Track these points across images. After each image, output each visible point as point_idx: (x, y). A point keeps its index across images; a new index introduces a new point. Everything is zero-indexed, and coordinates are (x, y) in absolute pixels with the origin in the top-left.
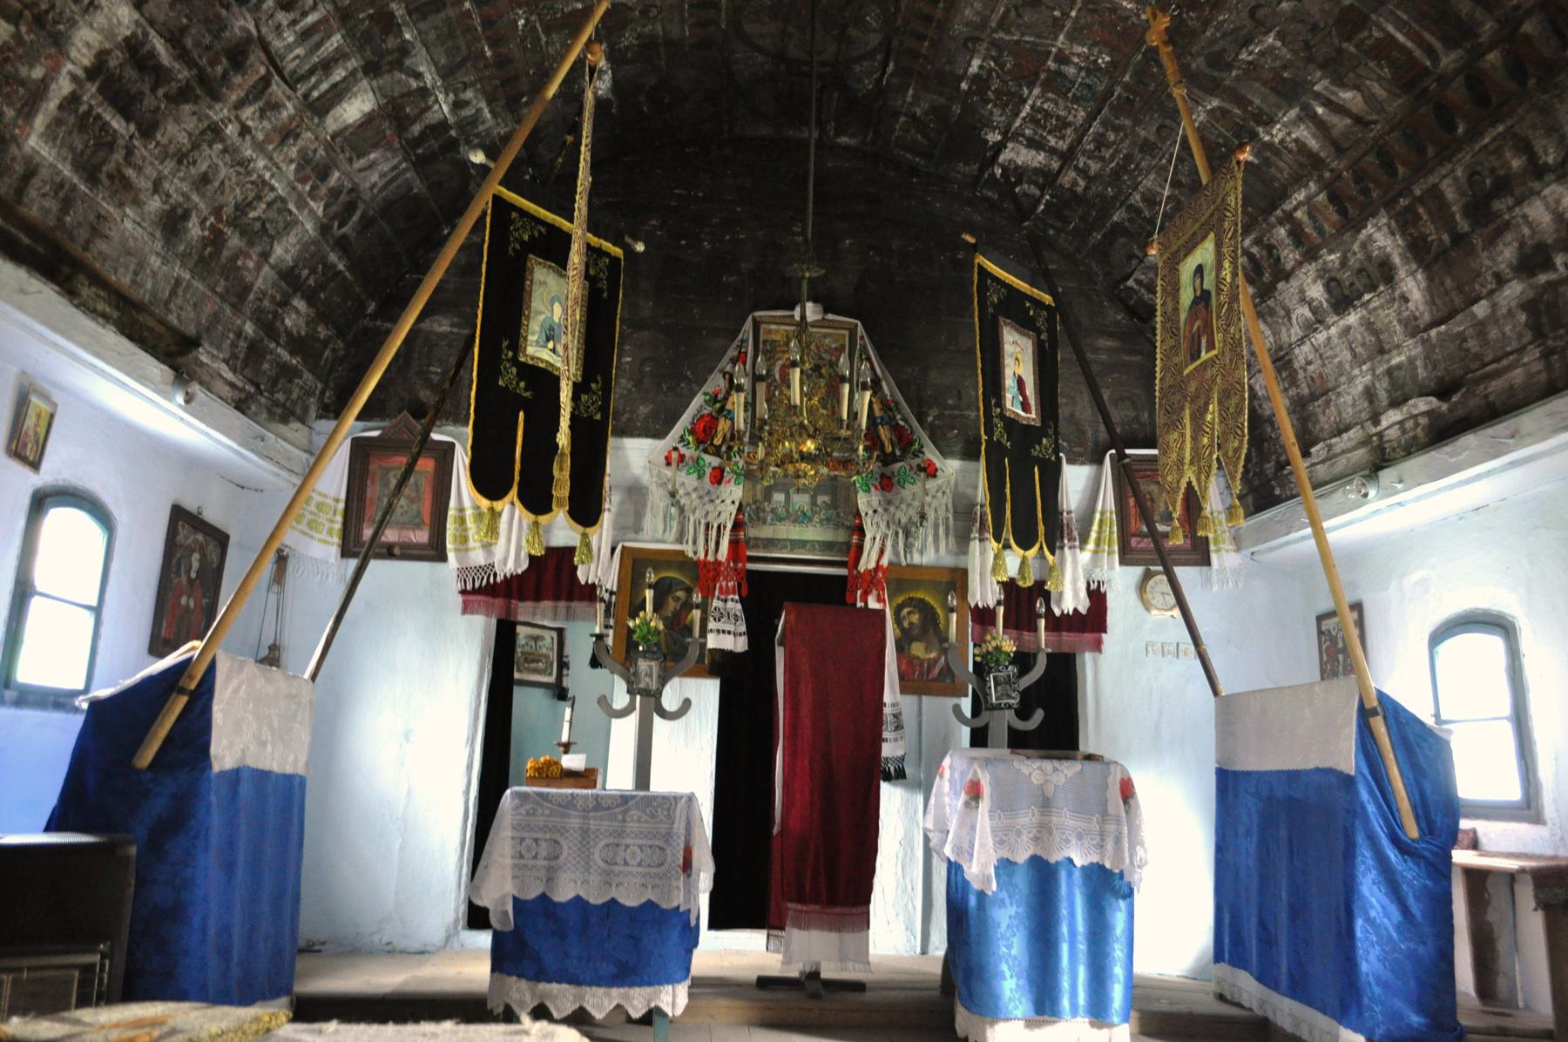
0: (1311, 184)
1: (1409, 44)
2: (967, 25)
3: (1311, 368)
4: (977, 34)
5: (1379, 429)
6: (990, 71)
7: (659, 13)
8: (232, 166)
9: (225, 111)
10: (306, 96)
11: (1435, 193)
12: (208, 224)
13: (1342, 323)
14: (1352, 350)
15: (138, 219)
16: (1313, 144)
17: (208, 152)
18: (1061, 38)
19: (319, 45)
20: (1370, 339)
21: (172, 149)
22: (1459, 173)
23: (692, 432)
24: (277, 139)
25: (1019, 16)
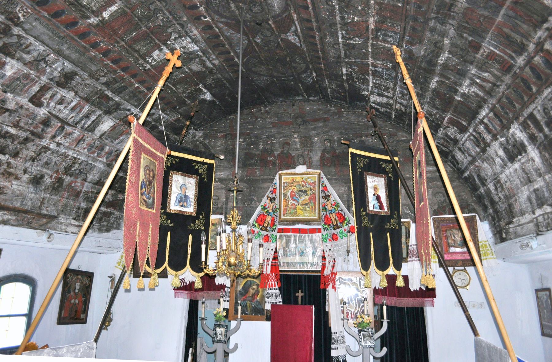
0: (486, 109)
1: (501, 54)
3: (507, 184)
5: (535, 216)
6: (351, 72)
8: (58, 157)
9: (47, 141)
10: (82, 128)
11: (532, 116)
12: (54, 177)
13: (513, 167)
14: (520, 179)
15: (19, 184)
16: (481, 93)
17: (45, 155)
18: (370, 58)
19: (80, 111)
20: (524, 175)
21: (28, 158)
22: (539, 108)
23: (256, 222)
24: (75, 143)
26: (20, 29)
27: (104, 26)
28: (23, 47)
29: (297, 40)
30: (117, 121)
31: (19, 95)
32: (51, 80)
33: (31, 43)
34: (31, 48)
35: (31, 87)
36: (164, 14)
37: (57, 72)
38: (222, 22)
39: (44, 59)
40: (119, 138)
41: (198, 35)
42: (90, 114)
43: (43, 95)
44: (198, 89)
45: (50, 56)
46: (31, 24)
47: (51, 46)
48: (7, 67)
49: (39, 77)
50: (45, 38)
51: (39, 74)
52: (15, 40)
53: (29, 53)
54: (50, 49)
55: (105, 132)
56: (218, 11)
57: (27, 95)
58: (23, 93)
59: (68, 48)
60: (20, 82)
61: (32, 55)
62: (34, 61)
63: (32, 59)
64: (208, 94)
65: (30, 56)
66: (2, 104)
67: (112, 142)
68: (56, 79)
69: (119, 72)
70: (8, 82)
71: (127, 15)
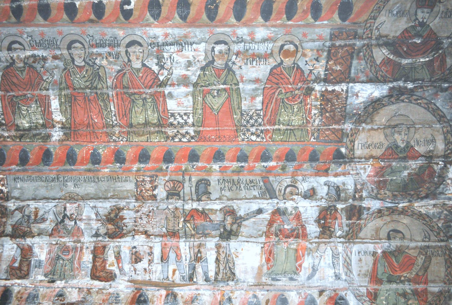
7: (291, 43)
10: (207, 280)
26: (13, 201)
27: (72, 129)
28: (33, 217)
30: (263, 239)
31: (74, 277)
32: (97, 235)
33: (36, 208)
34: (41, 213)
35: (80, 258)
36: (100, 55)
37: (94, 222)
39: (65, 216)
40: (300, 266)
41: (170, 31)
42: (199, 252)
43: (104, 261)
44: (322, 95)
45: (67, 209)
46: (16, 188)
47: (58, 196)
48: (36, 250)
49: (79, 242)
50: (42, 192)
51: (76, 238)
52: (18, 216)
53: (43, 220)
54: (60, 201)
55: (260, 268)
57: (83, 272)
58: (76, 272)
59: (75, 185)
60: (64, 260)
61: (49, 220)
62: (57, 225)
63: (53, 225)
64: (357, 87)
65: (48, 222)
66: (61, 300)
67: (291, 279)
68: (102, 231)
69: (167, 168)
70: (50, 268)
71: (75, 97)
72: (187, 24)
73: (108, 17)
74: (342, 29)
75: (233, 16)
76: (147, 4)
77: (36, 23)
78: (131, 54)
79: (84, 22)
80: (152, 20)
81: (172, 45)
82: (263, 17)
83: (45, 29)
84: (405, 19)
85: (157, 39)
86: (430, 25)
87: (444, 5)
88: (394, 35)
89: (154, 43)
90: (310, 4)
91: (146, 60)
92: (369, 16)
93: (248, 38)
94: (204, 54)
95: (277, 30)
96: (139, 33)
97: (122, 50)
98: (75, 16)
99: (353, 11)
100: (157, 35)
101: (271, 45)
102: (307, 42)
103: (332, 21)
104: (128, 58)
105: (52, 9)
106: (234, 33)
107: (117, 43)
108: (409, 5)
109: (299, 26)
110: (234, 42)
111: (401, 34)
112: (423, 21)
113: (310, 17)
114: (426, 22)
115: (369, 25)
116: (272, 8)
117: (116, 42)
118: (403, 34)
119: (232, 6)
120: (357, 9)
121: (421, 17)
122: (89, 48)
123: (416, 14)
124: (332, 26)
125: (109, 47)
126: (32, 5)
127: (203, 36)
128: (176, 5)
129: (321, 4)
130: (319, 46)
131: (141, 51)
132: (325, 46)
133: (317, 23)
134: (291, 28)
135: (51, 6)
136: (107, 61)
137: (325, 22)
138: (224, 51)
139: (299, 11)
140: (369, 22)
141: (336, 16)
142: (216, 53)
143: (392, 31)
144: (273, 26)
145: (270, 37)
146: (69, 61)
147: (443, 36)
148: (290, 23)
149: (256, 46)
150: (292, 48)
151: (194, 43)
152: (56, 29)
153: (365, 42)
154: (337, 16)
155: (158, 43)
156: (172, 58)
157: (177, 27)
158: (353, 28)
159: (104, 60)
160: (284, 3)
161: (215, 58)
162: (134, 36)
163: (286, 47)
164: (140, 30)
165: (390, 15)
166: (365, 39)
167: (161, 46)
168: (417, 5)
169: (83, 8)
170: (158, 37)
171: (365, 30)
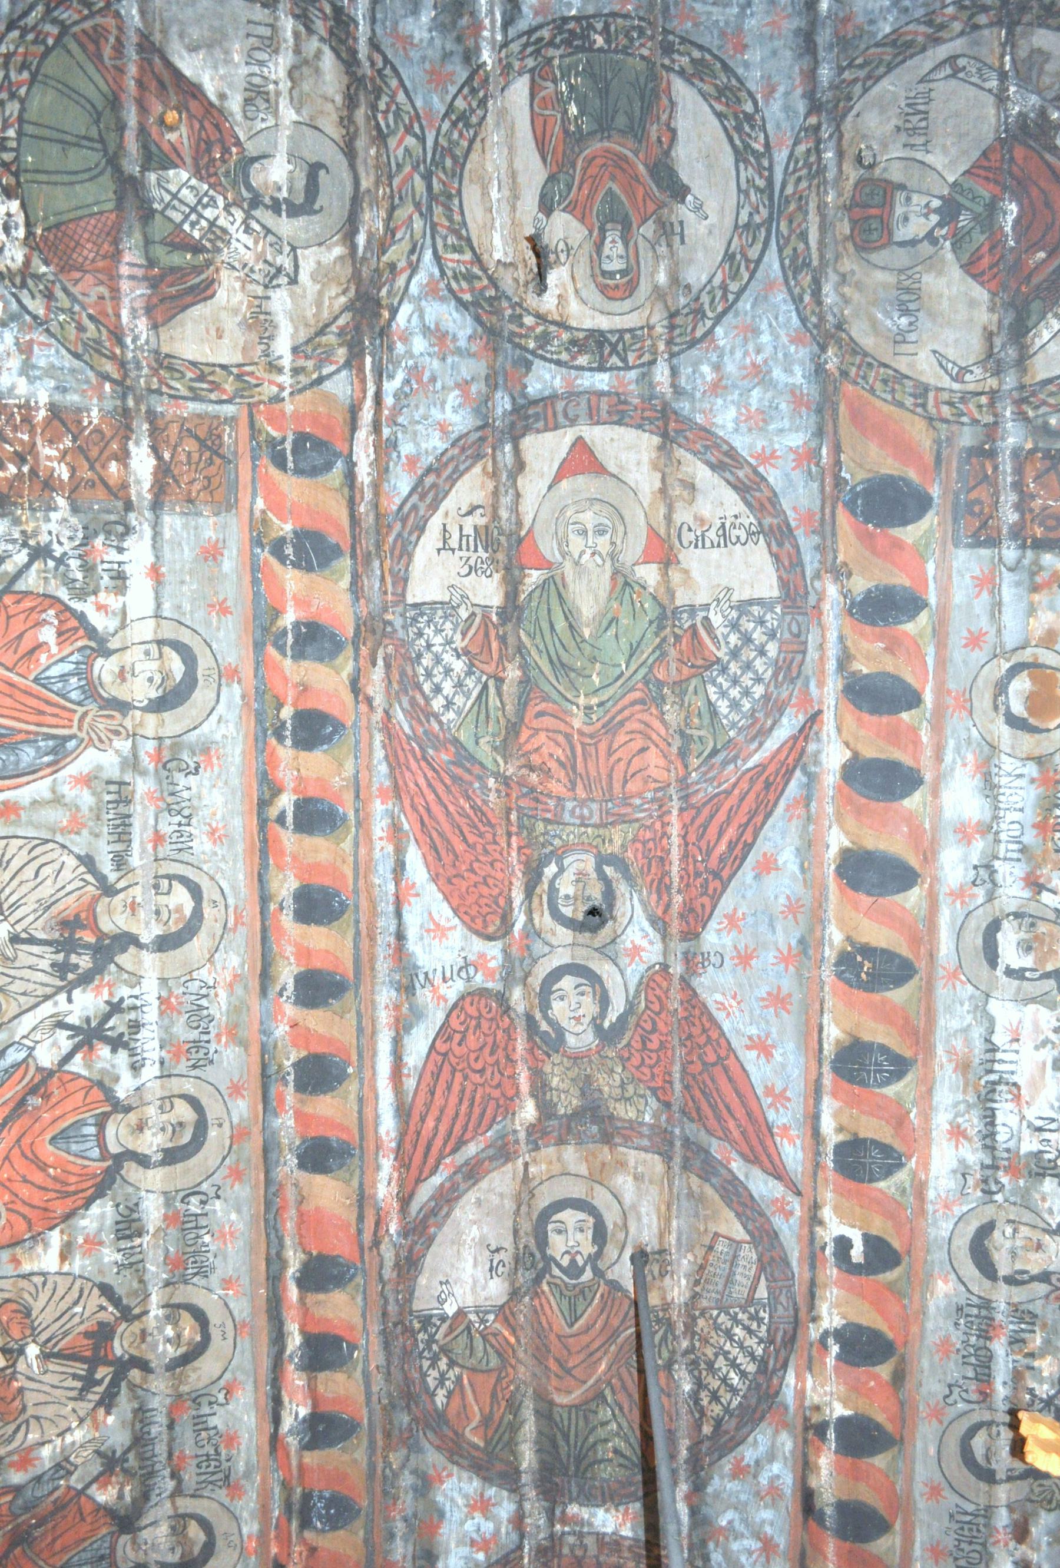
2: (206, 749)
4: (172, 723)
7: (1001, 688)
25: (88, 862)
29: (413, 919)
36: (1017, 1376)
38: (778, 1173)
41: (941, 1120)
56: (762, 1268)
72: (920, 1057)
73: (886, 1319)
74: (956, 505)
75: (899, 898)
76: (851, 1185)
77: (897, 1560)
78: (1018, 1266)
79: (902, 1404)
80: (902, 1176)
81: (993, 1116)
82: (907, 793)
83: (920, 1538)
84: (929, 281)
85: (967, 1167)
86: (951, 179)
87: (885, 146)
88: (984, 308)
89: (985, 1181)
90: (868, 629)
91: (1046, 1216)
92: (913, 412)
93: (979, 845)
94: (1032, 1008)
95: (951, 743)
96: (945, 1228)
97: (1002, 1296)
98: (878, 1426)
99: (895, 473)
100: (955, 1164)
101: (1008, 764)
102: (999, 631)
103: (927, 545)
104: (1033, 1279)
105: (853, 1497)
106: (959, 894)
107: (979, 1307)
108: (880, 276)
109: (942, 662)
110: (991, 898)
111: (982, 284)
112: (936, 211)
113: (909, 627)
114: (941, 198)
115: (946, 410)
116: (877, 760)
117: (975, 1311)
118: (983, 273)
119: (865, 900)
120: (890, 461)
121: (923, 220)
122: (990, 1408)
123: (913, 243)
124: (944, 543)
125: (990, 1339)
126: (838, 1555)
127: (966, 1007)
128: (857, 1089)
129: (869, 591)
130: (1018, 584)
131: (1009, 1231)
132: (1019, 561)
133: (933, 599)
134: (949, 692)
135: (844, 1498)
136: (1042, 1356)
137: (931, 568)
138: (1023, 935)
139: (889, 665)
140: (933, 411)
141: (910, 534)
142: (1028, 961)
143: (971, 320)
144: (939, 756)
145: (978, 767)
146: (1037, 1490)
147: (993, 120)
148: (928, 697)
149: (1012, 816)
150: (1021, 685)
151: (988, 1041)
152: (921, 1504)
153: (1008, 414)
154: (909, 528)
155: (983, 1167)
156: (1039, 1123)
157: (930, 1091)
158: (954, 464)
159: (1036, 1364)
160: (859, 719)
161: (1049, 967)
162: (956, 1243)
163: (1018, 708)
164: (935, 1222)
165: (912, 337)
166: (996, 415)
167: (994, 1158)
168: (883, 247)
169: (854, 1396)
170: (962, 1162)
171: (965, 419)
